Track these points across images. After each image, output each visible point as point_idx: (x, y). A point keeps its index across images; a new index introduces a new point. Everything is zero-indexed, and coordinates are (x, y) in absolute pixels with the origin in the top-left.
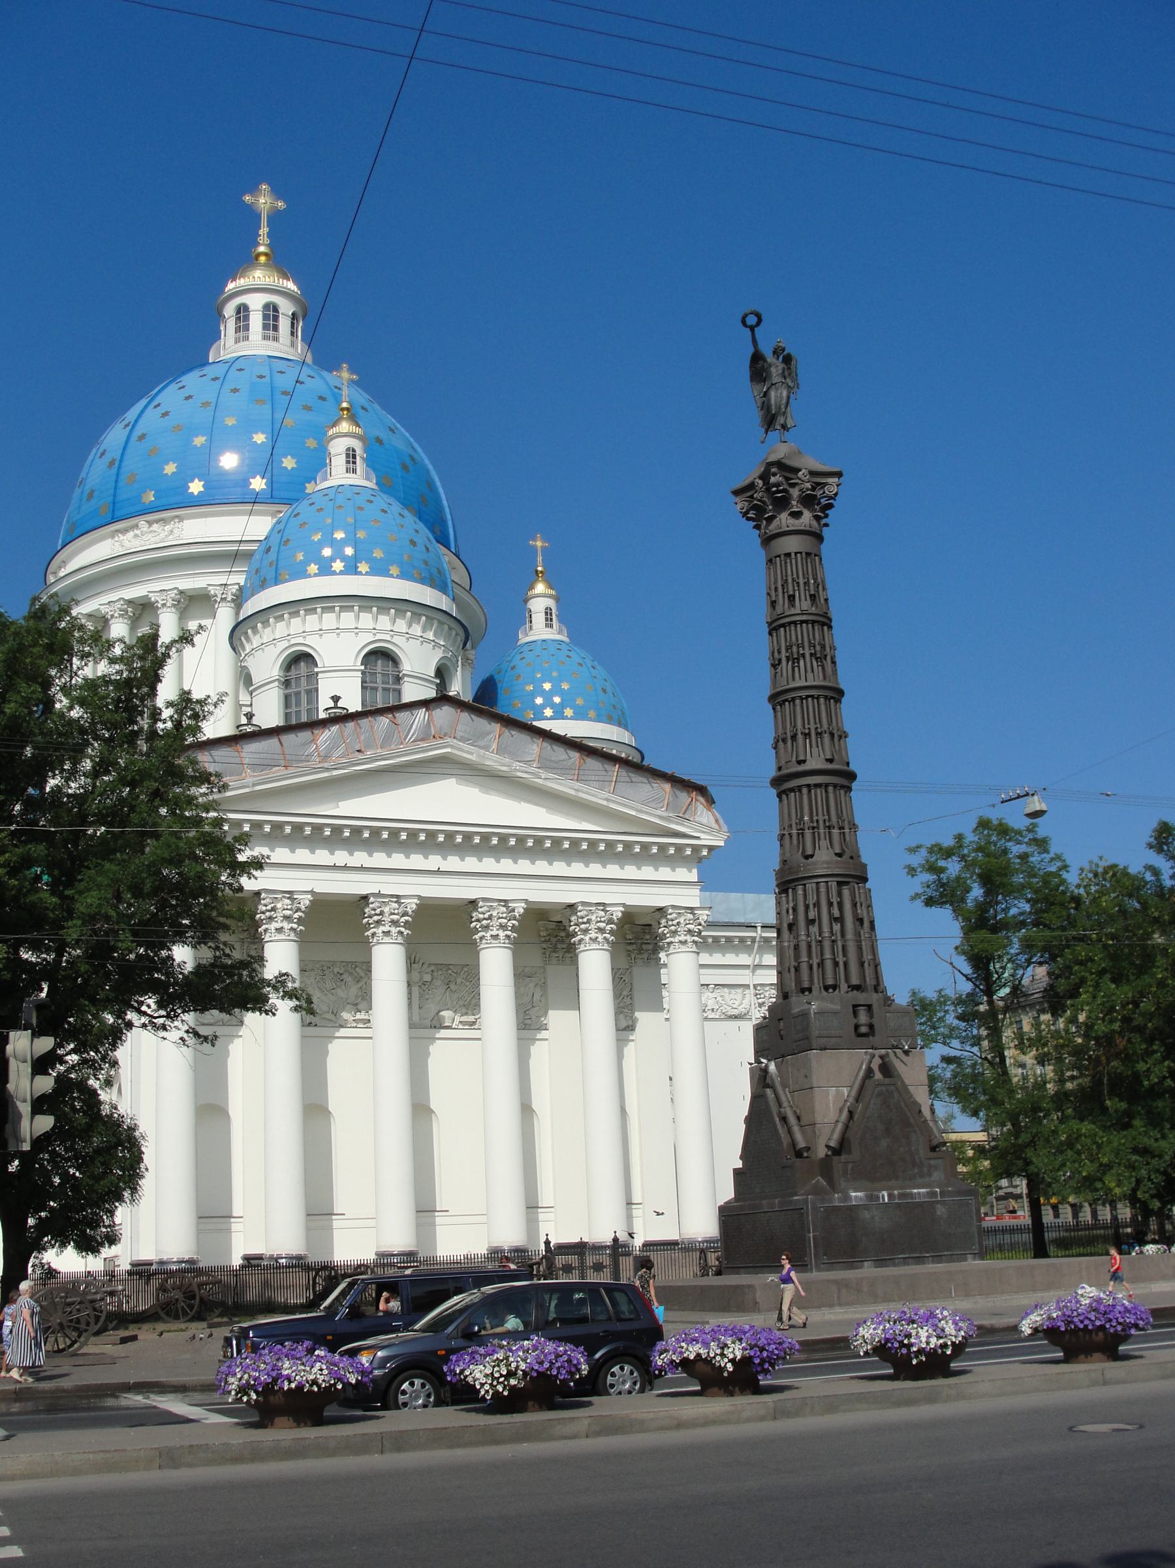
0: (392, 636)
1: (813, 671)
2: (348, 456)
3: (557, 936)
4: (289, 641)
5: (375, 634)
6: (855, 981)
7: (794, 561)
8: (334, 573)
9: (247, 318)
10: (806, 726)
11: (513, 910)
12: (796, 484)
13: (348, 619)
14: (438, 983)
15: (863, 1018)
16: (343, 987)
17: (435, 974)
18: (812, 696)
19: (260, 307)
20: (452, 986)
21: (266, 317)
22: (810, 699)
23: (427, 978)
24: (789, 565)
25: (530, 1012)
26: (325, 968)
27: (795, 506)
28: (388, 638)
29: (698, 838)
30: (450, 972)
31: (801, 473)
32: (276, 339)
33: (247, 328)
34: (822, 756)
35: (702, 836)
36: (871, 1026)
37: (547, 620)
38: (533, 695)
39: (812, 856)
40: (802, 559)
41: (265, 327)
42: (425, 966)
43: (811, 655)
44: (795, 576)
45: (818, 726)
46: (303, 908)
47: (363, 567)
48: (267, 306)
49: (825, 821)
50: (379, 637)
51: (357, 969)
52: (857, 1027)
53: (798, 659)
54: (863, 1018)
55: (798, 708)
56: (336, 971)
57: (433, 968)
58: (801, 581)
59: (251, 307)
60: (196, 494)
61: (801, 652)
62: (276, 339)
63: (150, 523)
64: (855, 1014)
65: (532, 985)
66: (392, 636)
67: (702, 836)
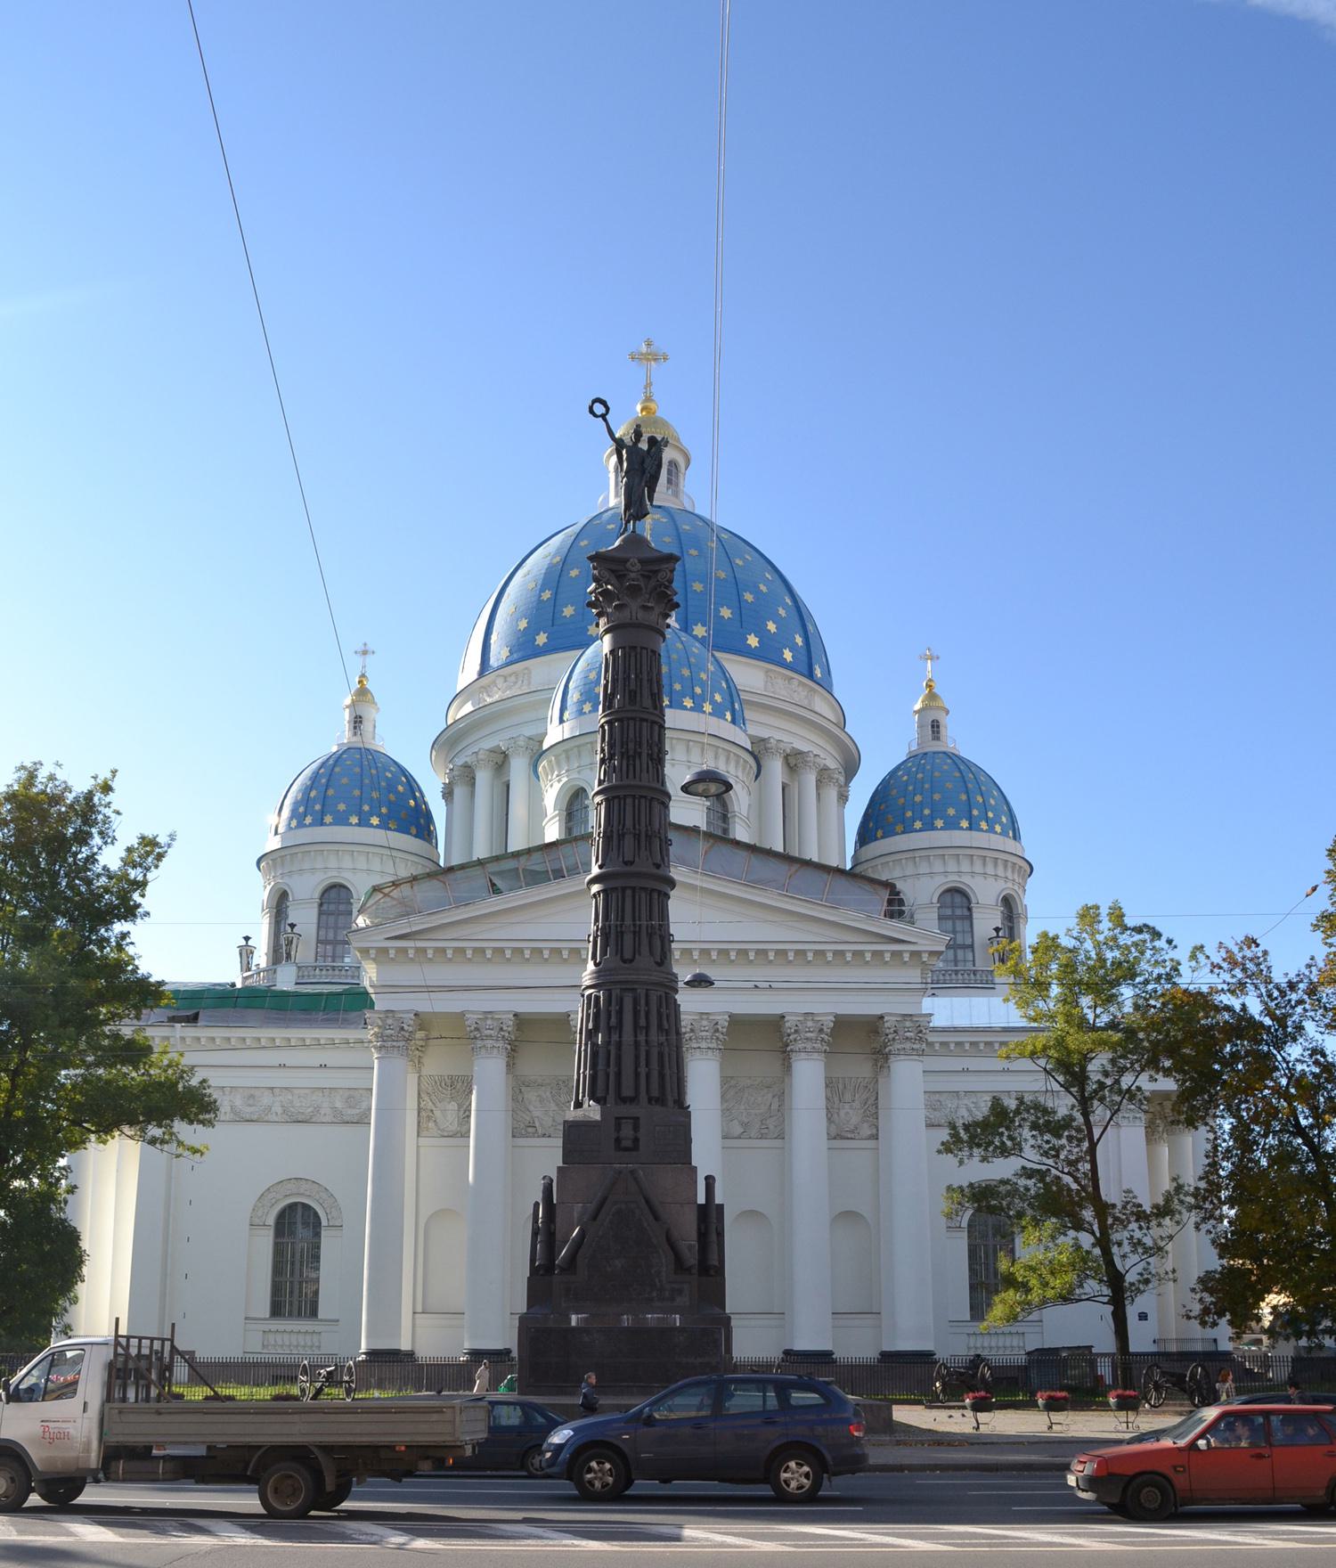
1: (648, 772)
4: (567, 776)
6: (655, 1093)
10: (637, 826)
11: (717, 1024)
15: (627, 1131)
18: (618, 797)
22: (643, 801)
25: (768, 1122)
26: (560, 1083)
34: (621, 859)
35: (920, 941)
36: (636, 1140)
37: (933, 732)
38: (904, 809)
39: (631, 961)
44: (638, 671)
45: (621, 827)
49: (616, 926)
52: (618, 1140)
54: (627, 1131)
55: (629, 809)
58: (645, 677)
61: (639, 750)
64: (618, 1127)
65: (770, 1095)
67: (920, 941)
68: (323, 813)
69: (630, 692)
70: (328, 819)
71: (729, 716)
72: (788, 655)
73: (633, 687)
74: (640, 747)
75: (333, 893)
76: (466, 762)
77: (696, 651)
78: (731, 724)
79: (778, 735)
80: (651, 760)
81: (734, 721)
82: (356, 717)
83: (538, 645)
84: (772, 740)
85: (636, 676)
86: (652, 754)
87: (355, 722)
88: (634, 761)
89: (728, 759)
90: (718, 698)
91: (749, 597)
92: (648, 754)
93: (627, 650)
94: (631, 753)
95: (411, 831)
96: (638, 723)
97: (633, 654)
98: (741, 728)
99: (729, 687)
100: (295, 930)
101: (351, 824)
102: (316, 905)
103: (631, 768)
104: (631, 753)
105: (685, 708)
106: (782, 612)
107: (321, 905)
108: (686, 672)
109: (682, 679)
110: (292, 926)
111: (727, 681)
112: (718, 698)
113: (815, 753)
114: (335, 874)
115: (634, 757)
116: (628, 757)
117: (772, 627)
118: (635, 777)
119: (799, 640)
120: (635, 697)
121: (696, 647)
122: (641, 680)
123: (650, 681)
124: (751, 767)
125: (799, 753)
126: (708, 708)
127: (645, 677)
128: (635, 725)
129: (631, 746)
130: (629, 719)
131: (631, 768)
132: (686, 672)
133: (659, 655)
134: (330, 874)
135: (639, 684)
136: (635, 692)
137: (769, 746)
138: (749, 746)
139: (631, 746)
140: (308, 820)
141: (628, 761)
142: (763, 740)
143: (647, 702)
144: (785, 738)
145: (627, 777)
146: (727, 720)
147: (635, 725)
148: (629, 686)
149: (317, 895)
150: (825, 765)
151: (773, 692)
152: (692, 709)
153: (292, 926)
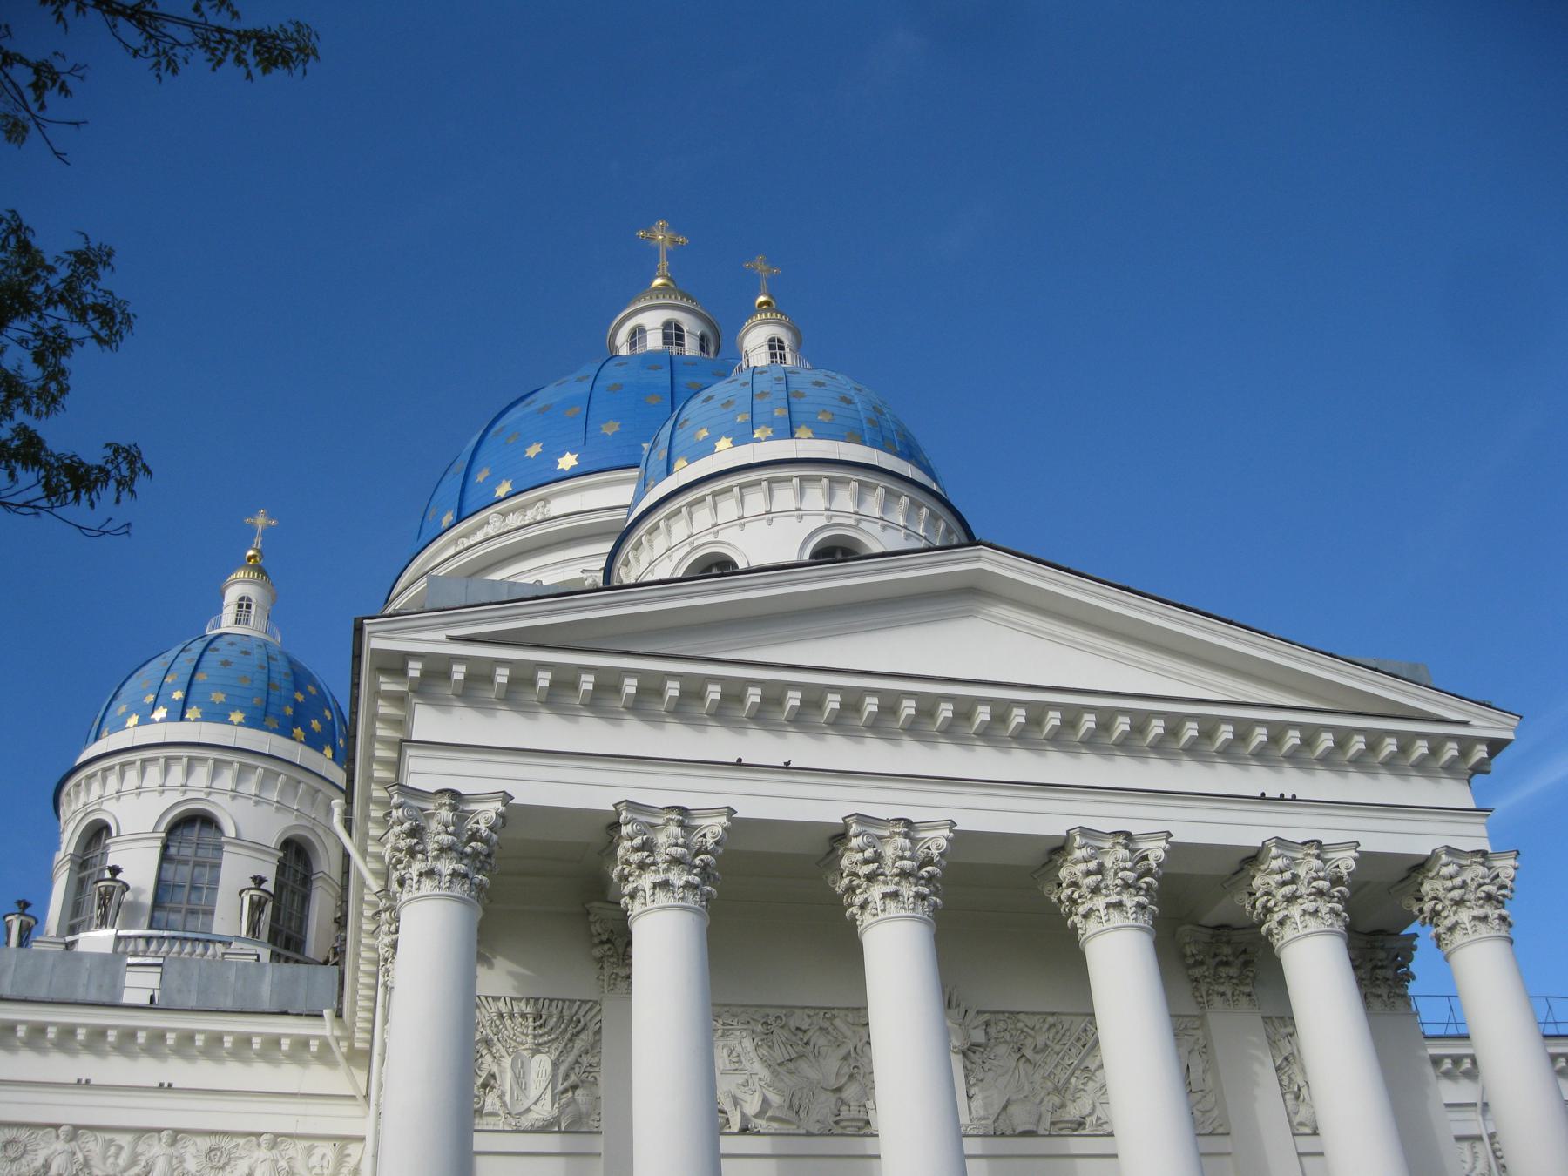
0: (859, 521)
2: (771, 347)
3: (1216, 955)
5: (831, 517)
11: (1146, 858)
13: (785, 497)
14: (1002, 1050)
16: (811, 1056)
17: (993, 1031)
19: (659, 325)
20: (1028, 1052)
23: (978, 1036)
26: (771, 1020)
29: (1465, 723)
30: (1020, 1025)
42: (971, 1014)
46: (710, 841)
48: (667, 325)
51: (837, 1022)
56: (793, 1023)
57: (986, 1017)
60: (568, 453)
63: (504, 514)
68: (185, 703)
70: (192, 713)
75: (194, 833)
82: (242, 599)
83: (563, 470)
87: (240, 606)
95: (325, 752)
100: (119, 877)
101: (232, 723)
102: (159, 844)
107: (165, 847)
110: (115, 870)
114: (202, 795)
134: (189, 795)
140: (160, 713)
149: (163, 827)
153: (115, 870)
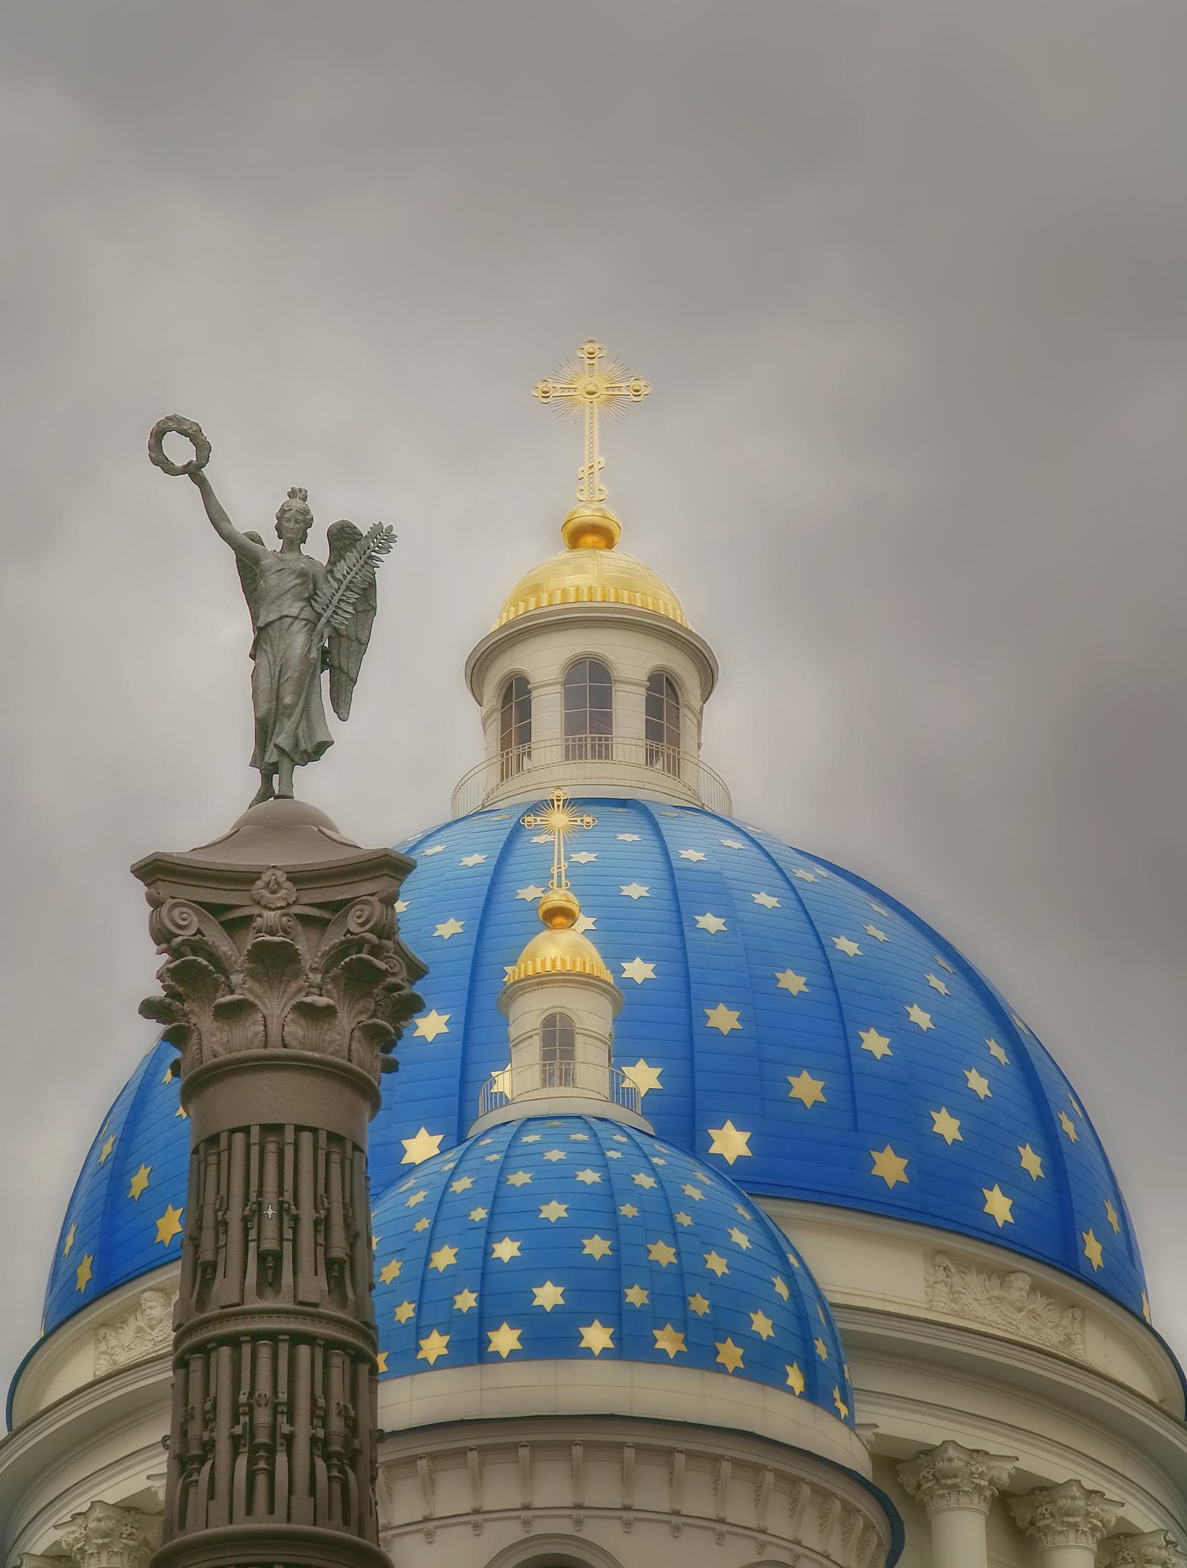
0: (578, 1522)
7: (289, 1152)
8: (424, 1367)
9: (525, 711)
12: (251, 918)
21: (571, 697)
24: (212, 1170)
27: (241, 987)
28: (566, 1527)
31: (259, 883)
32: (603, 752)
33: (525, 735)
40: (248, 1146)
41: (572, 725)
43: (236, 1441)
44: (288, 1196)
47: (505, 1339)
50: (540, 1528)
53: (202, 1460)
58: (307, 1213)
59: (535, 678)
61: (286, 1429)
62: (603, 752)
66: (578, 1522)
69: (262, 1257)
71: (795, 1379)
72: (999, 1206)
73: (270, 1244)
74: (291, 1421)
76: (57, 1543)
77: (695, 1193)
78: (806, 1406)
79: (972, 1437)
80: (327, 1457)
81: (814, 1393)
84: (952, 1452)
85: (281, 1209)
86: (326, 1442)
88: (271, 1461)
89: (794, 1502)
90: (762, 1325)
91: (876, 1043)
92: (314, 1440)
93: (255, 1132)
94: (262, 1438)
96: (283, 1349)
97: (271, 1147)
98: (836, 1413)
99: (795, 1295)
103: (261, 1481)
104: (262, 1438)
105: (661, 1358)
106: (978, 1083)
108: (663, 1253)
109: (652, 1274)
111: (790, 1277)
112: (762, 1325)
113: (1089, 1486)
115: (271, 1451)
116: (254, 1450)
117: (947, 1126)
118: (271, 1510)
119: (1031, 1162)
120: (278, 1270)
121: (698, 1184)
122: (296, 1219)
123: (322, 1224)
124: (868, 1526)
125: (1044, 1489)
126: (730, 1353)
127: (307, 1213)
128: (275, 1357)
129: (263, 1416)
130: (256, 1336)
131: (261, 1481)
132: (663, 1253)
133: (357, 1148)
135: (288, 1234)
136: (278, 1257)
137: (941, 1465)
138: (864, 1467)
139: (263, 1416)
141: (252, 1462)
142: (928, 1452)
143: (314, 1286)
144: (995, 1443)
145: (249, 1510)
146: (790, 1390)
147: (275, 1357)
148: (258, 1240)
150: (1121, 1520)
151: (955, 1314)
152: (681, 1361)
